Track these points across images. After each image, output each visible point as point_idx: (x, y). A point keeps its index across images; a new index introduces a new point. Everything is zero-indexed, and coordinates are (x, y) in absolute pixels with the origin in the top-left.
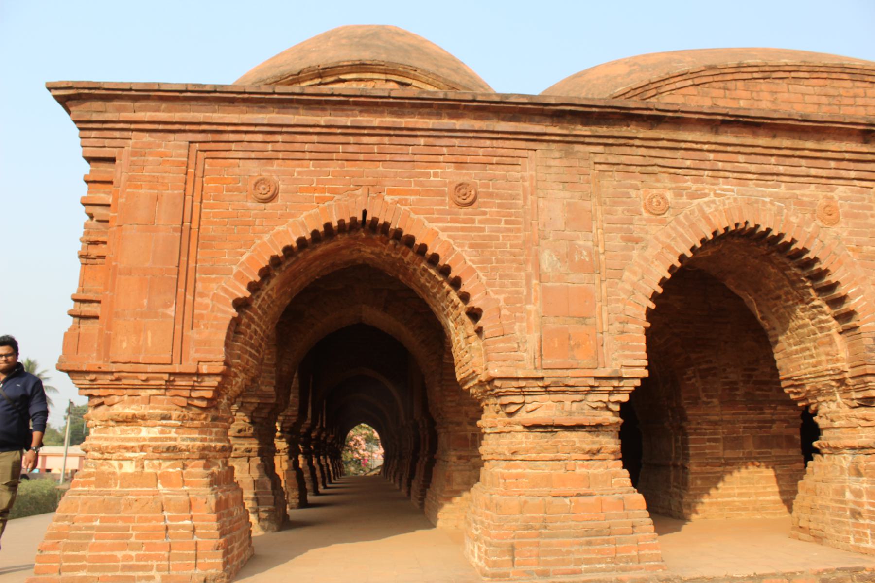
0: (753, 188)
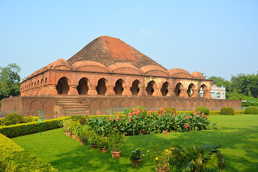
0: (85, 75)
